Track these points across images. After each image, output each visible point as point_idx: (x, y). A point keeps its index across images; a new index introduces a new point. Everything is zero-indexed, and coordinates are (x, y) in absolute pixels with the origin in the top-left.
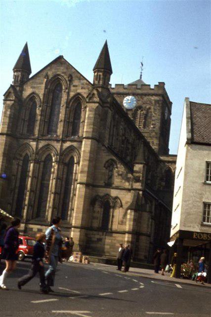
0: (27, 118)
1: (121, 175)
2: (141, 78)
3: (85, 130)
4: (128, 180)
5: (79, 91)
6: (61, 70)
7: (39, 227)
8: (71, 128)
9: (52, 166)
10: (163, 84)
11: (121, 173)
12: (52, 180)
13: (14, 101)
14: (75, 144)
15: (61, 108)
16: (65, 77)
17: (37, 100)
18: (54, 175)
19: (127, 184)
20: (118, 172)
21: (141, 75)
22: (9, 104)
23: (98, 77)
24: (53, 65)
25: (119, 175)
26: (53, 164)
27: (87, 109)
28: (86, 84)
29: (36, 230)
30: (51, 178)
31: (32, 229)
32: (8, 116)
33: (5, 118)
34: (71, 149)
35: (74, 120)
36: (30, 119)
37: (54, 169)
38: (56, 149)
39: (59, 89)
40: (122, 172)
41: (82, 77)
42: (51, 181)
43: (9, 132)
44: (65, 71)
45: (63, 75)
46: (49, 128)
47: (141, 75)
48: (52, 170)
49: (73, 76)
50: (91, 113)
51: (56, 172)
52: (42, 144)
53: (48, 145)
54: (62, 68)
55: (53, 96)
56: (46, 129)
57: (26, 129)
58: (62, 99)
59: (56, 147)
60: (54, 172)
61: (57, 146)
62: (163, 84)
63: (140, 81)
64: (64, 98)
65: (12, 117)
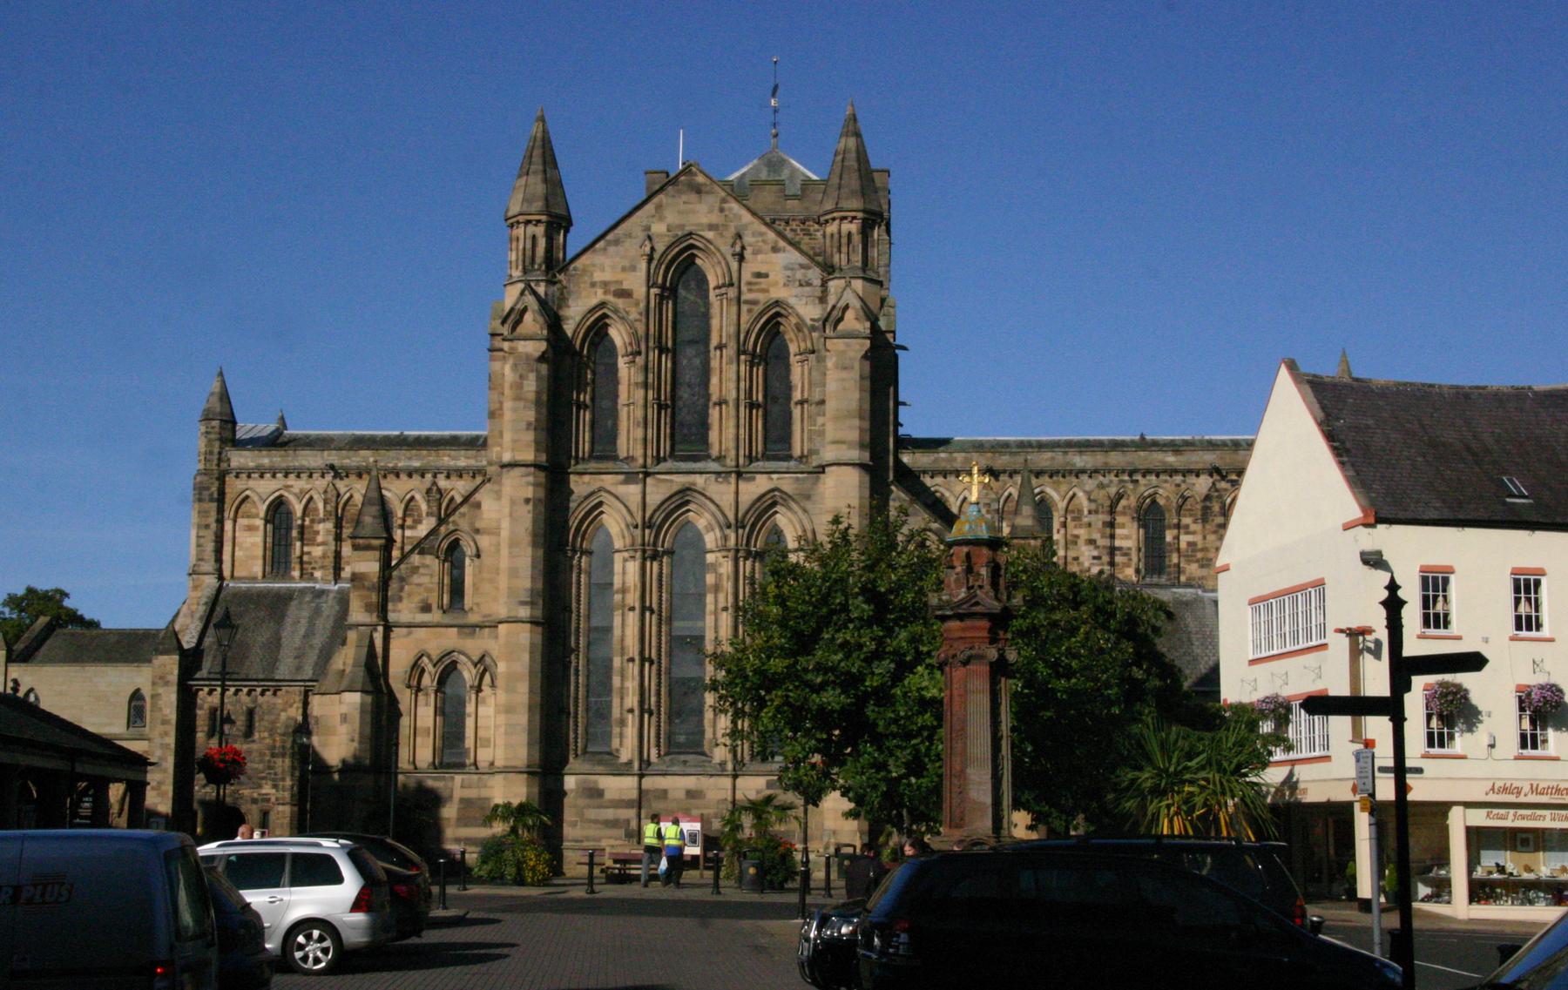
3: (830, 433)
5: (778, 293)
7: (690, 782)
9: (704, 567)
12: (716, 613)
13: (548, 340)
14: (787, 483)
15: (715, 355)
16: (719, 242)
17: (618, 335)
18: (721, 597)
22: (528, 357)
23: (844, 240)
24: (661, 198)
26: (710, 558)
27: (830, 363)
28: (802, 266)
29: (682, 795)
30: (710, 607)
31: (665, 792)
32: (532, 396)
33: (521, 404)
37: (719, 576)
41: (782, 243)
42: (709, 620)
44: (715, 218)
45: (710, 235)
46: (672, 427)
48: (710, 579)
49: (748, 239)
50: (844, 374)
51: (728, 586)
52: (657, 492)
53: (686, 490)
54: (702, 208)
56: (666, 430)
58: (715, 323)
59: (714, 497)
60: (717, 588)
61: (723, 493)
64: (722, 323)
65: (545, 397)
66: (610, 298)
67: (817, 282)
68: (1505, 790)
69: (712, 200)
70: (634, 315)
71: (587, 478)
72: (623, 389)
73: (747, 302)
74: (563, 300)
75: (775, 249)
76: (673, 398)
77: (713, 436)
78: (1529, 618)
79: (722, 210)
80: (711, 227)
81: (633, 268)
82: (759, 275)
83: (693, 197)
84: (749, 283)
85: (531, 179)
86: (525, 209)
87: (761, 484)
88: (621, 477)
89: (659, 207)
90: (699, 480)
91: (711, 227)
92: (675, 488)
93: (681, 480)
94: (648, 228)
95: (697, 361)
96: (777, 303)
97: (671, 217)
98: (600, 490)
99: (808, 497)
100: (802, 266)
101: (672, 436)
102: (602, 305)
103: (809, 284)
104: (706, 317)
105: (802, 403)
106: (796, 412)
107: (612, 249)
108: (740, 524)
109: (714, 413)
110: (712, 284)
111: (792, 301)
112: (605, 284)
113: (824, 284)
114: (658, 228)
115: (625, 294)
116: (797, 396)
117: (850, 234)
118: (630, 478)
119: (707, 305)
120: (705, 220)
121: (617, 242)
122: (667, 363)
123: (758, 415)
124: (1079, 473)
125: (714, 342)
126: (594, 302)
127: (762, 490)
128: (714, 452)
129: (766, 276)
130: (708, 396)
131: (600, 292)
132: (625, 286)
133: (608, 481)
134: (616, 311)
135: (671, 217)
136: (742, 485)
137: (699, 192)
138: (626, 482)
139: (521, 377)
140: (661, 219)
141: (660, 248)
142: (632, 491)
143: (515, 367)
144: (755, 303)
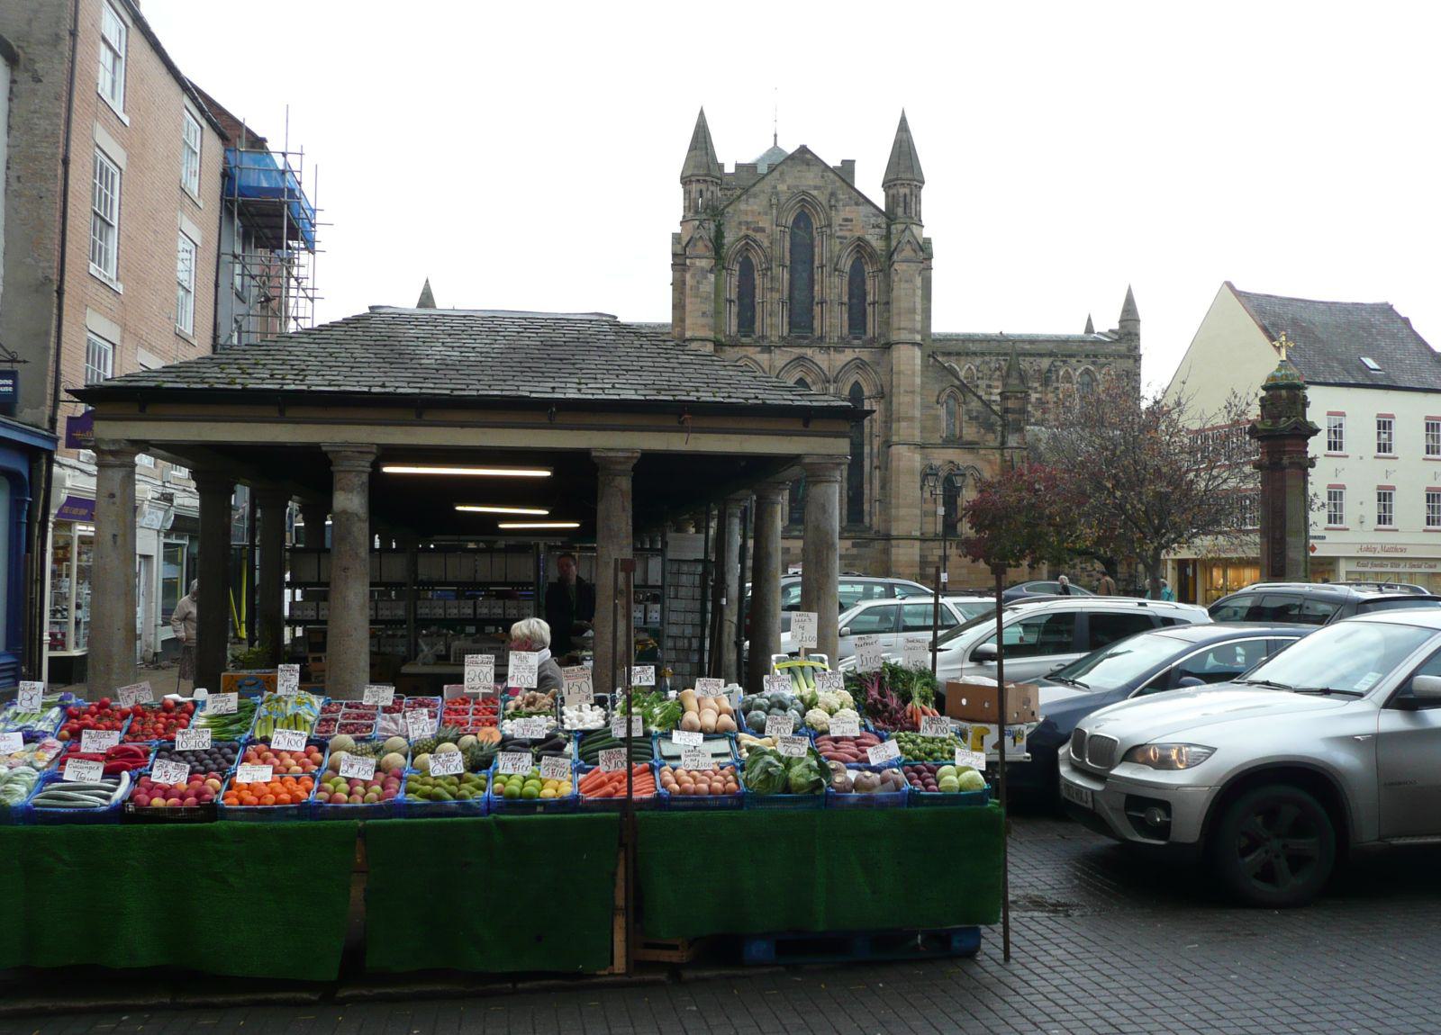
0: (734, 296)
1: (976, 418)
2: (775, 143)
4: (990, 428)
6: (809, 179)
8: (846, 316)
10: (854, 161)
11: (975, 414)
19: (990, 436)
20: (969, 412)
21: (776, 136)
23: (902, 199)
25: (971, 418)
34: (860, 365)
35: (850, 299)
36: (741, 296)
38: (820, 368)
39: (802, 225)
40: (978, 411)
41: (861, 200)
43: (711, 335)
44: (819, 182)
45: (815, 193)
46: (790, 317)
47: (776, 136)
53: (801, 358)
54: (810, 175)
55: (792, 244)
56: (786, 320)
57: (734, 322)
59: (819, 363)
62: (854, 161)
63: (776, 149)
64: (822, 251)
66: (750, 233)
67: (884, 226)
68: (1368, 549)
69: (816, 169)
70: (766, 243)
71: (736, 349)
72: (758, 292)
73: (838, 237)
74: (719, 234)
75: (857, 204)
76: (791, 297)
77: (817, 323)
78: (1385, 445)
79: (823, 177)
80: (816, 188)
81: (766, 214)
82: (846, 220)
83: (805, 167)
84: (840, 225)
85: (698, 153)
86: (696, 172)
87: (849, 355)
88: (759, 349)
89: (782, 174)
90: (809, 352)
91: (816, 188)
92: (793, 357)
93: (797, 351)
94: (775, 187)
95: (805, 275)
96: (859, 239)
97: (790, 181)
98: (746, 356)
99: (878, 364)
100: (874, 215)
101: (790, 323)
102: (747, 236)
103: (880, 228)
104: (812, 247)
105: (874, 303)
106: (869, 310)
107: (751, 200)
108: (835, 382)
109: (817, 309)
110: (814, 227)
111: (868, 237)
112: (747, 223)
113: (889, 227)
114: (782, 187)
115: (762, 230)
116: (870, 299)
117: (905, 195)
118: (767, 349)
119: (812, 239)
120: (811, 183)
121: (755, 196)
122: (786, 276)
123: (845, 308)
124: (975, 354)
125: (817, 263)
126: (742, 234)
127: (849, 359)
128: (817, 333)
129: (851, 220)
130: (813, 298)
131: (744, 228)
132: (761, 225)
133: (751, 351)
134: (755, 241)
135: (790, 181)
136: (838, 356)
137: (808, 164)
138: (762, 352)
139: (698, 282)
140: (784, 181)
141: (783, 199)
142: (763, 358)
143: (693, 276)
144: (846, 238)
